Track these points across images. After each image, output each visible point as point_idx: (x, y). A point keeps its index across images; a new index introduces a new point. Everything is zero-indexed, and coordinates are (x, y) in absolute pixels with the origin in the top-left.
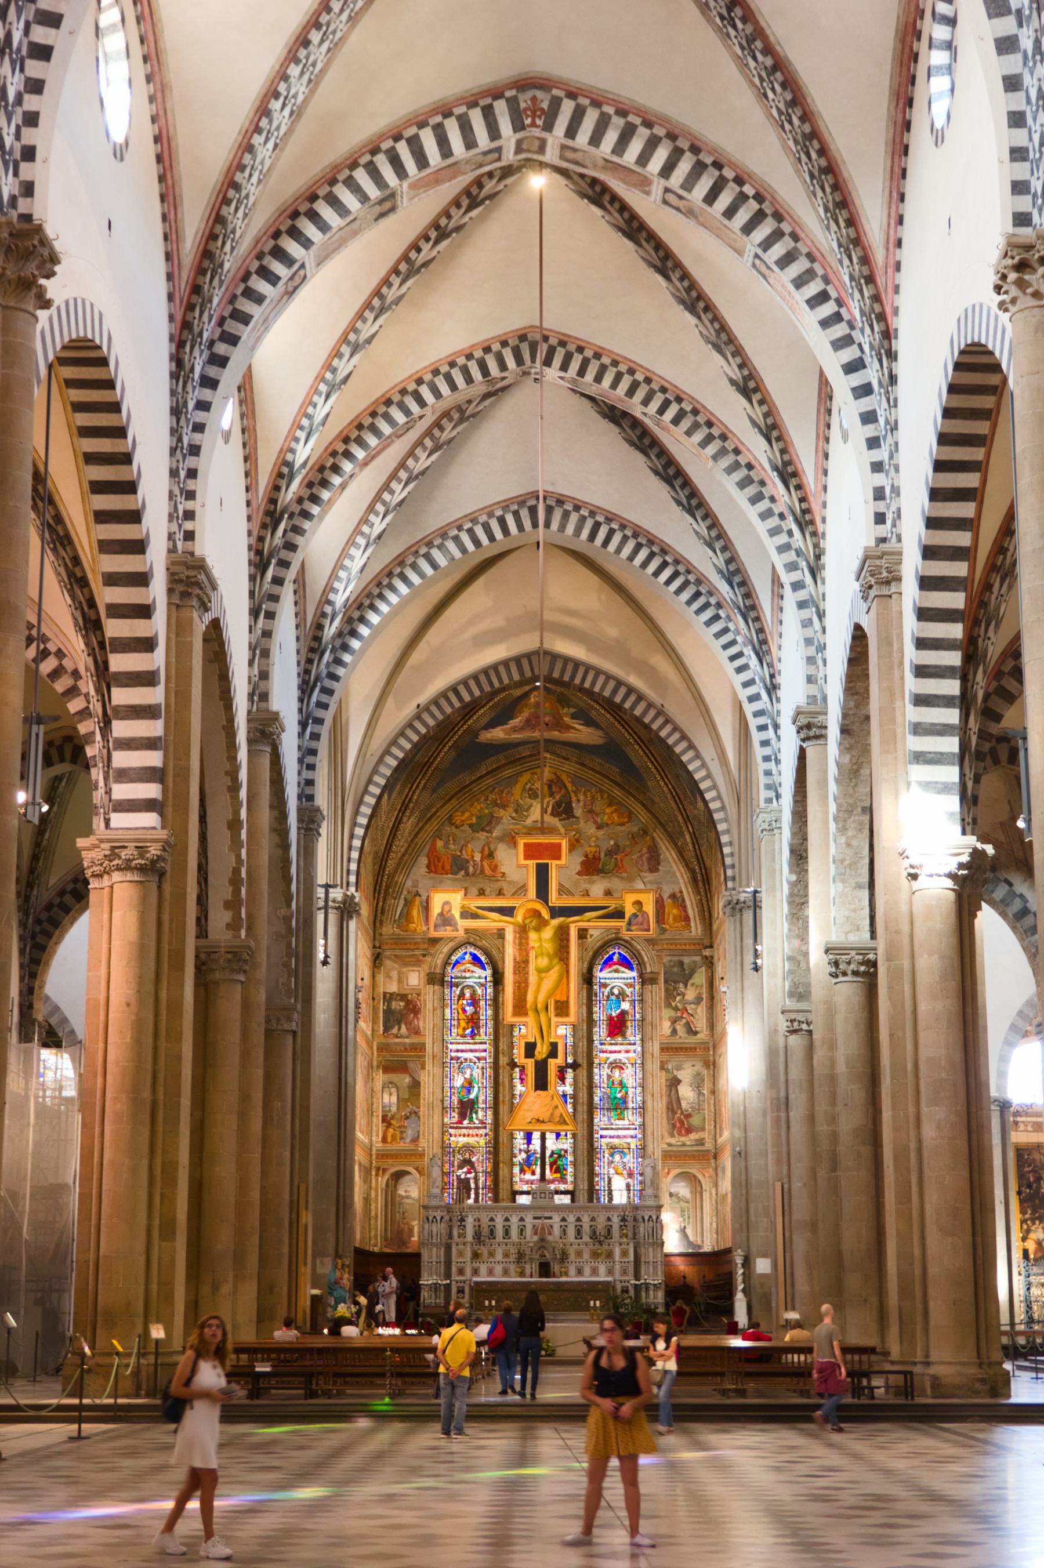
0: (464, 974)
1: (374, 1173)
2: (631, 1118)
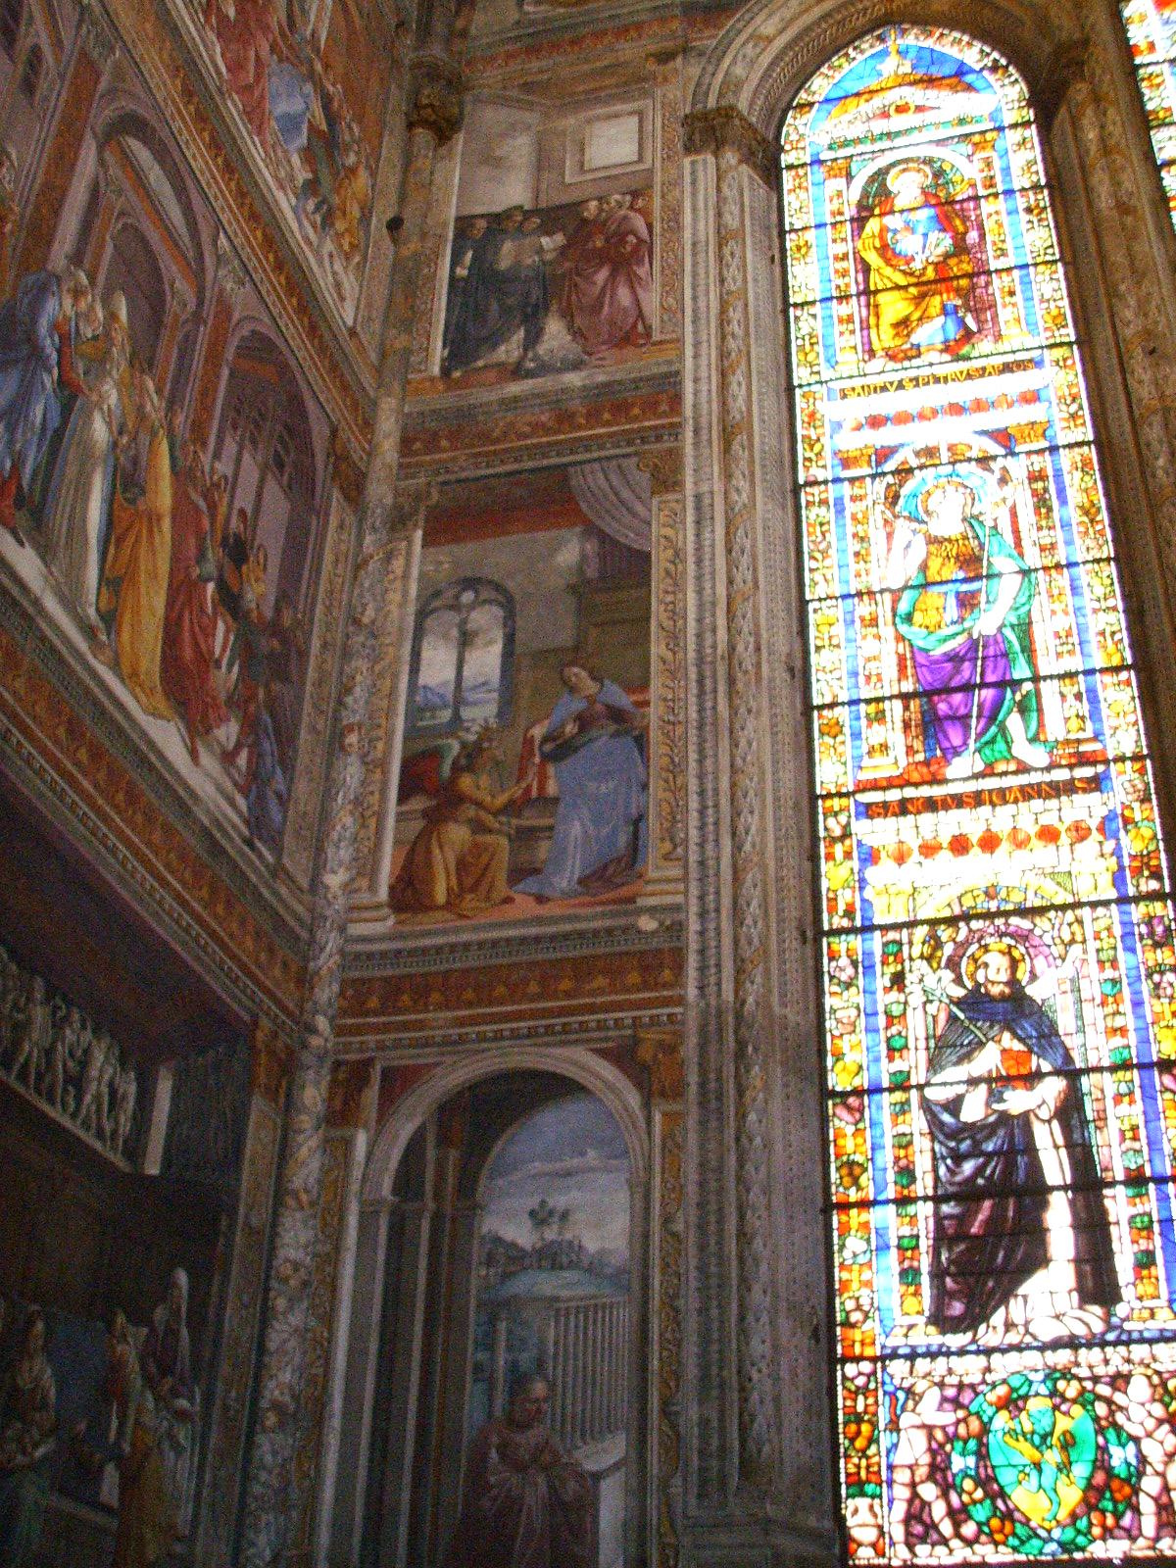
0: (879, 126)
1: (313, 1095)
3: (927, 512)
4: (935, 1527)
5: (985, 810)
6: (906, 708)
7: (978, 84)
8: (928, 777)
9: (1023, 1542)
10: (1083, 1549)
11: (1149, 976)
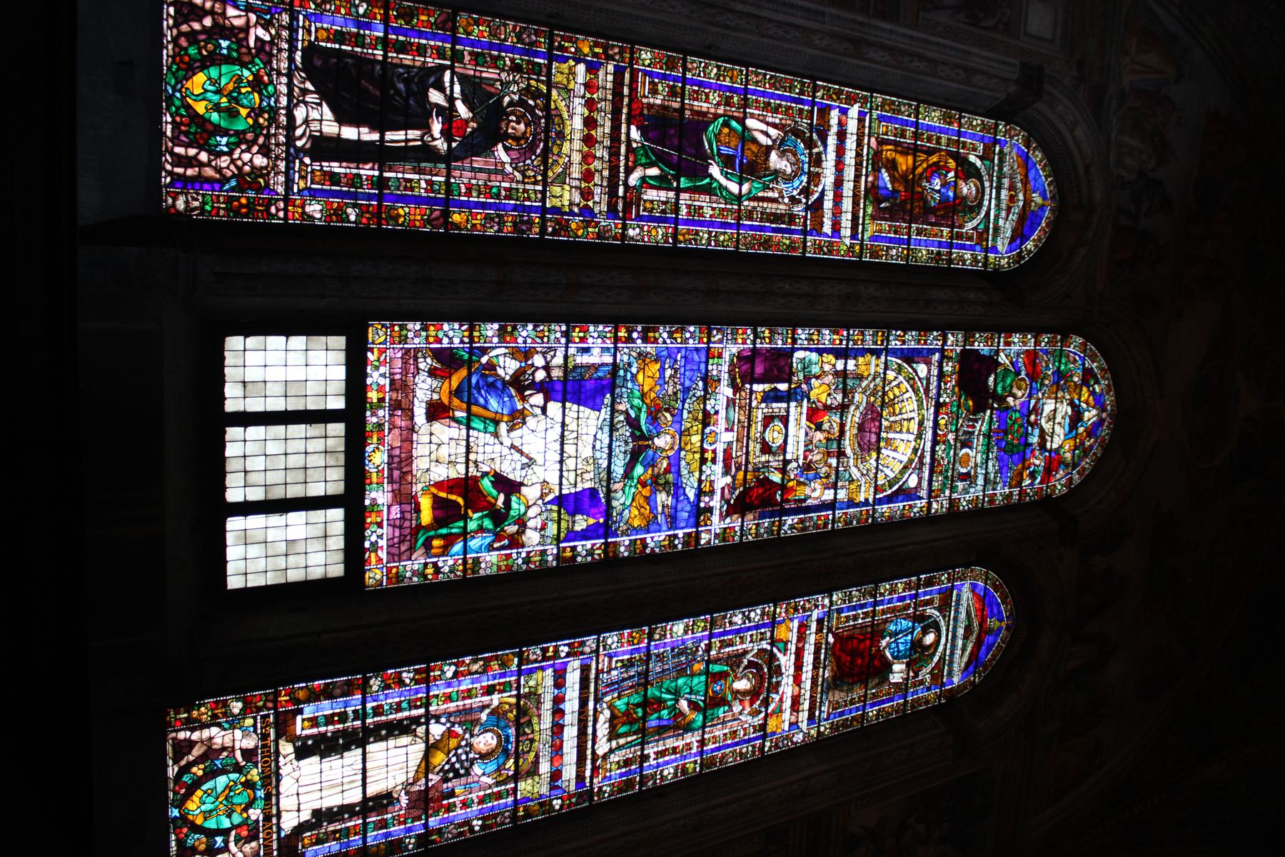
0: (1006, 182)
2: (614, 758)
3: (785, 151)
4: (186, 22)
5: (607, 143)
6: (675, 110)
7: (1014, 245)
8: (633, 113)
9: (173, 74)
10: (168, 109)
11: (498, 216)
